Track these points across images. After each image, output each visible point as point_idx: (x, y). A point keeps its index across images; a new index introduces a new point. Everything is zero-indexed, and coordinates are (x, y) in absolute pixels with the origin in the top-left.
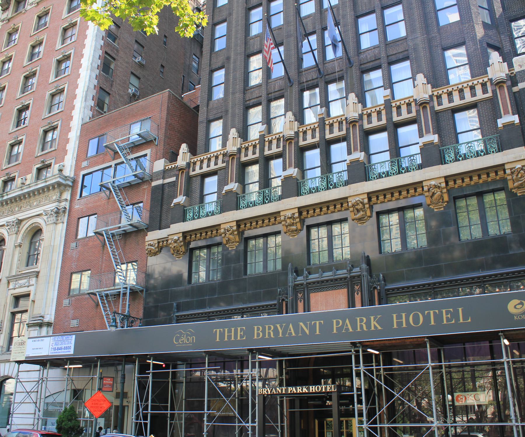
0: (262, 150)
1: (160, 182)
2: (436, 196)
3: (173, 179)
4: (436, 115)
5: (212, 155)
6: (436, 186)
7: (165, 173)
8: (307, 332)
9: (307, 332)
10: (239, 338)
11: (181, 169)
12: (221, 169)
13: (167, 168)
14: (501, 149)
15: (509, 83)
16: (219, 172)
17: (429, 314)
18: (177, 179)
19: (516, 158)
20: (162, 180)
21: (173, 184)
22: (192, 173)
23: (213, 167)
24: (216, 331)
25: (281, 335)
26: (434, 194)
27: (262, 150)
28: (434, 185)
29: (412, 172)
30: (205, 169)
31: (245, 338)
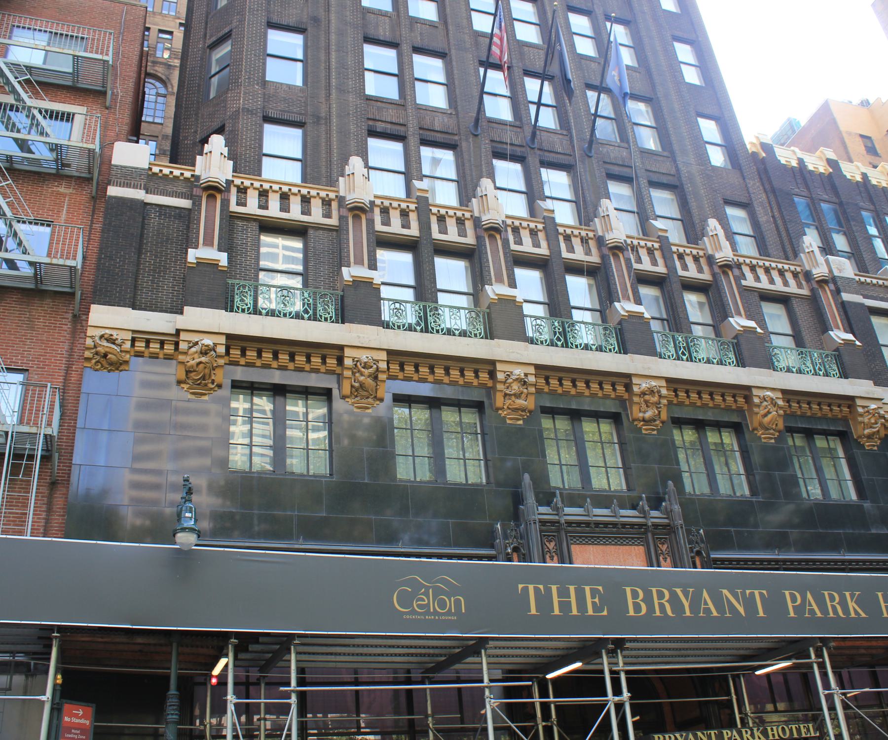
0: (425, 226)
1: (138, 194)
2: (770, 416)
3: (185, 203)
4: (746, 291)
5: (257, 184)
6: (773, 402)
7: (151, 180)
8: (741, 610)
9: (741, 610)
10: (590, 612)
11: (213, 190)
12: (318, 227)
13: (156, 169)
14: (844, 375)
15: (832, 287)
16: (311, 232)
17: (752, 594)
18: (197, 204)
19: (868, 393)
20: (143, 192)
21: (187, 218)
22: (234, 207)
23: (295, 213)
24: (526, 590)
25: (688, 613)
26: (769, 412)
27: (425, 226)
28: (772, 399)
29: (728, 368)
30: (274, 210)
31: (605, 613)
